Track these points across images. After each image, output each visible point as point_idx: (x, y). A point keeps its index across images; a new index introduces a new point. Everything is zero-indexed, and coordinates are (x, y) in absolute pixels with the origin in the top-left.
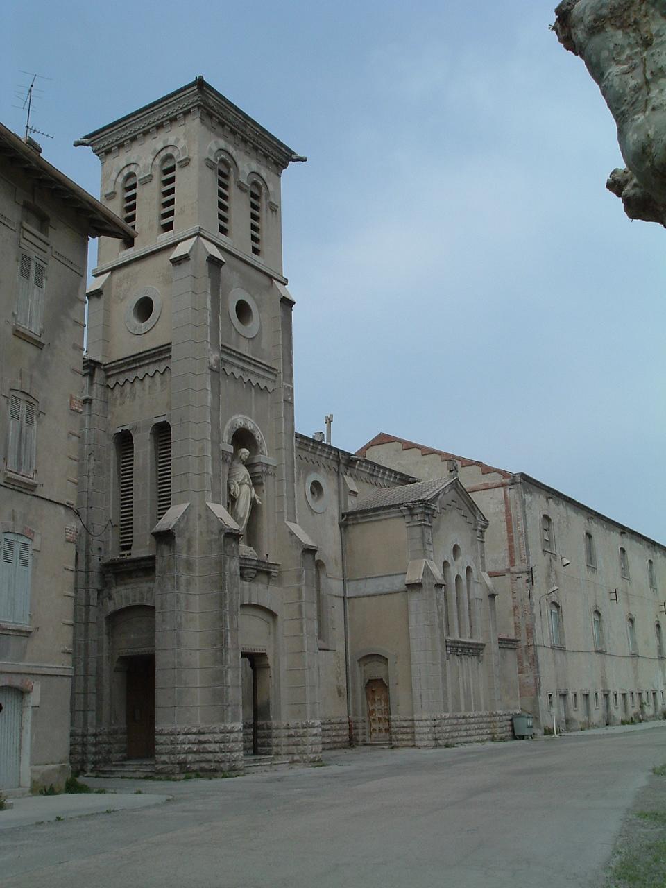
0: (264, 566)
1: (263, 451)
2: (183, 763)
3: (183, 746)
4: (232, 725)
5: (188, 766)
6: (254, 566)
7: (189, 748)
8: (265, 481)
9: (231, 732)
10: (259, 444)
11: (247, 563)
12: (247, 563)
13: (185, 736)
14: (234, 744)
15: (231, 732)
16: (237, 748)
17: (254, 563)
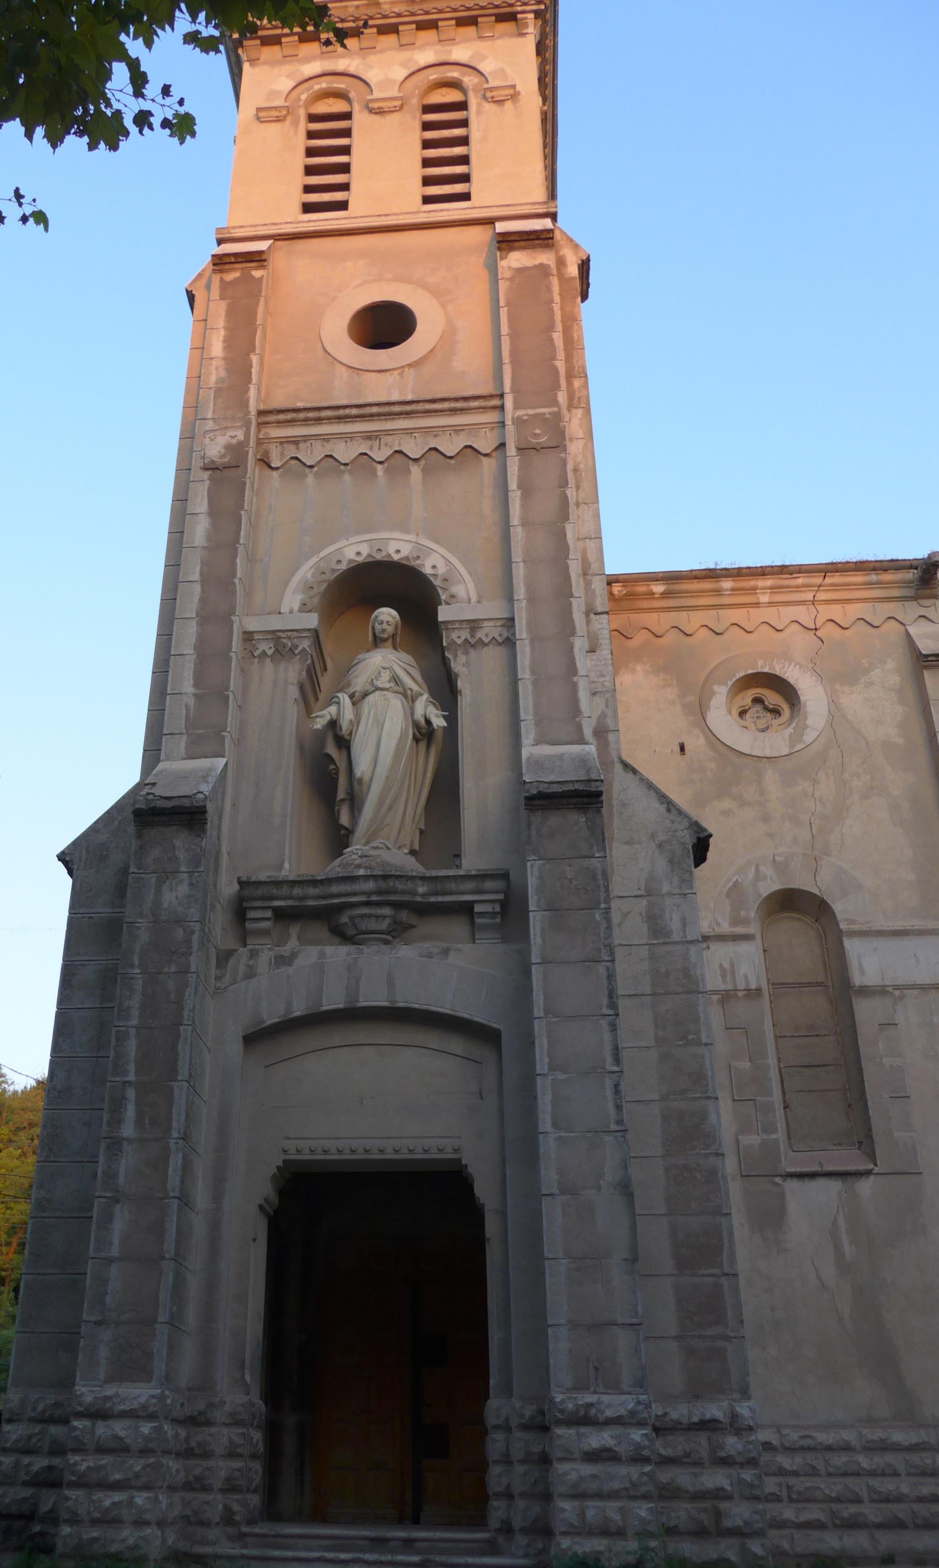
0: (421, 890)
1: (453, 596)
2: (20, 1517)
3: (26, 1460)
4: (110, 1391)
5: (37, 1528)
6: (369, 894)
7: (50, 1468)
8: (467, 664)
9: (99, 1414)
10: (437, 582)
11: (335, 889)
12: (335, 889)
13: (38, 1428)
14: (105, 1460)
15: (99, 1414)
16: (118, 1476)
17: (370, 885)
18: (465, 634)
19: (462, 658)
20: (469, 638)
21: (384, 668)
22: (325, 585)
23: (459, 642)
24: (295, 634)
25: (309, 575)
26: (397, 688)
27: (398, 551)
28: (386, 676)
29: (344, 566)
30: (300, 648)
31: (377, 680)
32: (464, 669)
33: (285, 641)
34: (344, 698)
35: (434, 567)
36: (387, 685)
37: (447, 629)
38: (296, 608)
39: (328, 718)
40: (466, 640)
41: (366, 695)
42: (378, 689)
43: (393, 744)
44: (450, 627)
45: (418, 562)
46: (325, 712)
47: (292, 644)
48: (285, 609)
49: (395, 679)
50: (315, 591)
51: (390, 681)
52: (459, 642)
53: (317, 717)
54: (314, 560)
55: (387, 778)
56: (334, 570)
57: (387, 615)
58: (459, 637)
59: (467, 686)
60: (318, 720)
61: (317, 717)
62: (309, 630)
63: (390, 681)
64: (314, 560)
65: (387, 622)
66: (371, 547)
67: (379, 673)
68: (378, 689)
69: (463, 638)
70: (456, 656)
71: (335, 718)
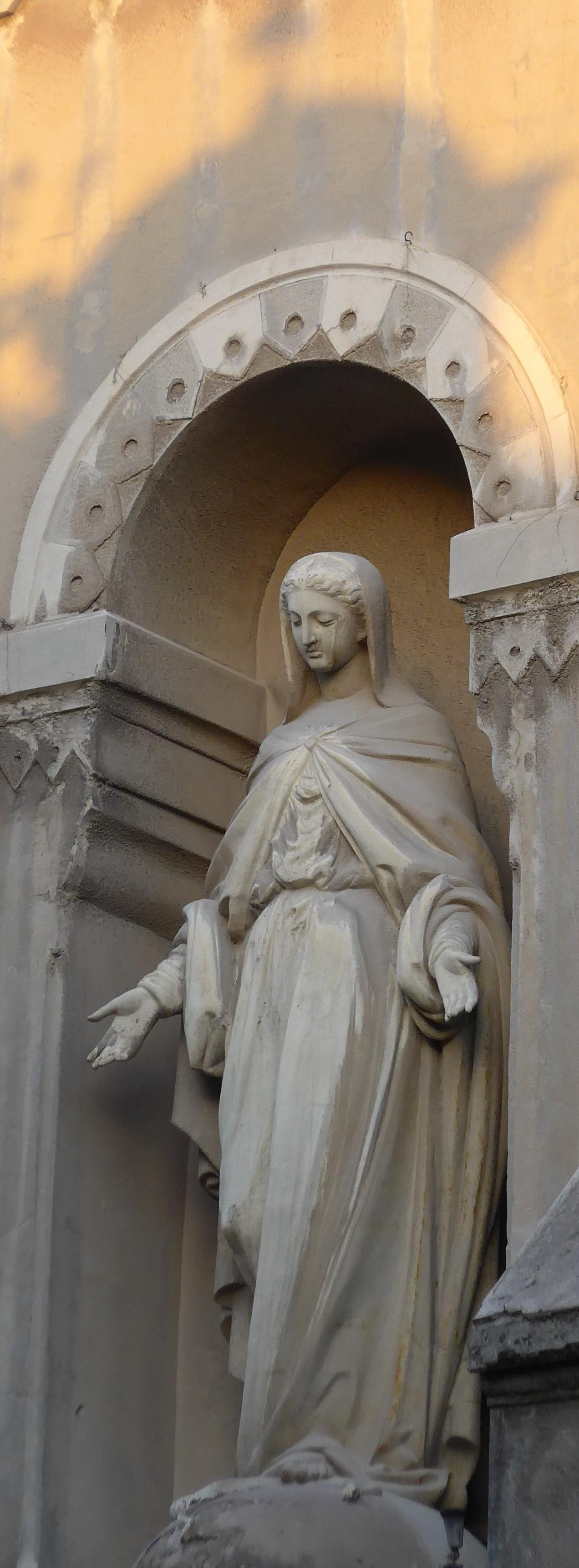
18: (532, 637)
19: (525, 735)
20: (544, 652)
21: (304, 800)
22: (134, 492)
23: (515, 668)
24: (47, 704)
25: (90, 458)
26: (350, 869)
27: (349, 317)
28: (312, 826)
29: (188, 408)
30: (63, 756)
31: (284, 849)
32: (530, 776)
33: (20, 733)
34: (200, 924)
35: (453, 367)
36: (309, 868)
37: (480, 624)
38: (53, 599)
39: (149, 1009)
40: (536, 659)
41: (256, 909)
42: (283, 886)
43: (324, 1092)
44: (489, 614)
45: (407, 354)
46: (137, 992)
47: (42, 743)
48: (20, 608)
49: (338, 839)
50: (109, 520)
51: (322, 848)
52: (515, 668)
53: (114, 1012)
54: (107, 390)
55: (315, 1217)
56: (162, 425)
57: (323, 577)
58: (515, 651)
59: (536, 843)
60: (118, 1022)
61: (114, 1012)
62: (83, 683)
63: (322, 848)
64: (107, 390)
65: (314, 615)
66: (270, 313)
67: (293, 819)
68: (283, 886)
69: (527, 654)
70: (506, 727)
71: (172, 1004)
